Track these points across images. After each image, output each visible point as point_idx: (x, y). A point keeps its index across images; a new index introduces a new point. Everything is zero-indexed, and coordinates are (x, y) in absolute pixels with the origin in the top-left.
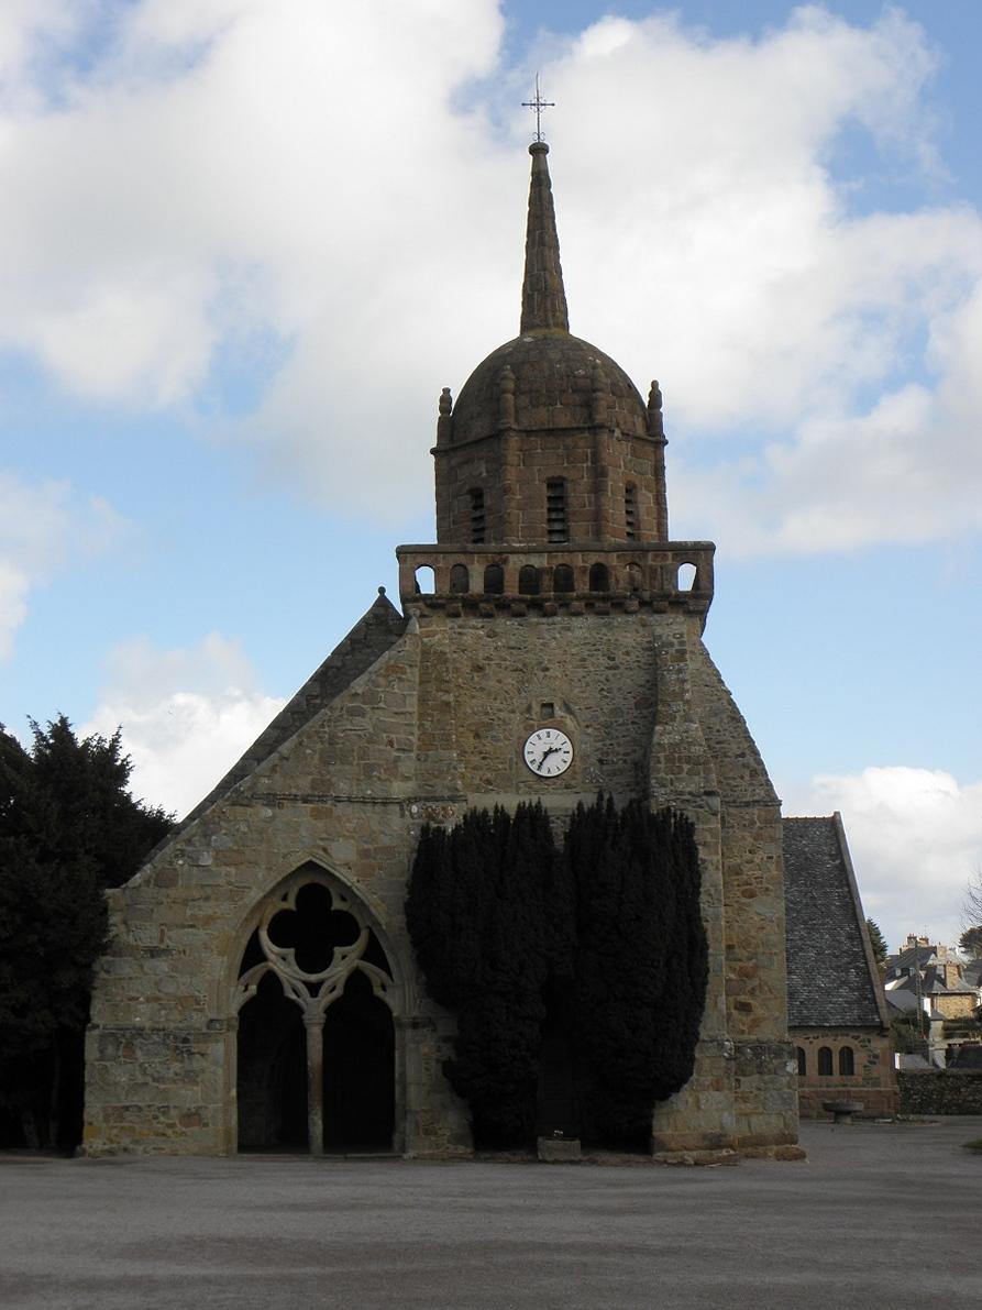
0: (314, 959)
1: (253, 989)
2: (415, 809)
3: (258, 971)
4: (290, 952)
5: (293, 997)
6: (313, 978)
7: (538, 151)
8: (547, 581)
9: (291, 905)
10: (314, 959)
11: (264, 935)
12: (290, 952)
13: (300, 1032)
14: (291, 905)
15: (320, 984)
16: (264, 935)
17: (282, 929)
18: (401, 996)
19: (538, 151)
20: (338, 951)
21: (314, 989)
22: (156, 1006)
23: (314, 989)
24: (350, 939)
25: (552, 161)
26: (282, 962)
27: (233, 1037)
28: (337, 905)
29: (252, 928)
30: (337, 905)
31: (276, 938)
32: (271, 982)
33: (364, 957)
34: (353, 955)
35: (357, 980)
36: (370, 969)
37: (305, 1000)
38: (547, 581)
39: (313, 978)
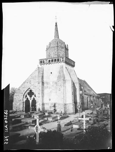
0: (31, 97)
3: (26, 98)
6: (31, 98)
7: (56, 24)
8: (51, 61)
9: (29, 92)
10: (31, 97)
14: (29, 92)
17: (28, 94)
19: (56, 24)
21: (31, 99)
22: (19, 100)
23: (31, 99)
24: (33, 95)
26: (28, 97)
27: (24, 103)
28: (32, 92)
30: (32, 92)
31: (28, 95)
36: (35, 97)
37: (30, 100)
38: (51, 61)
39: (31, 98)
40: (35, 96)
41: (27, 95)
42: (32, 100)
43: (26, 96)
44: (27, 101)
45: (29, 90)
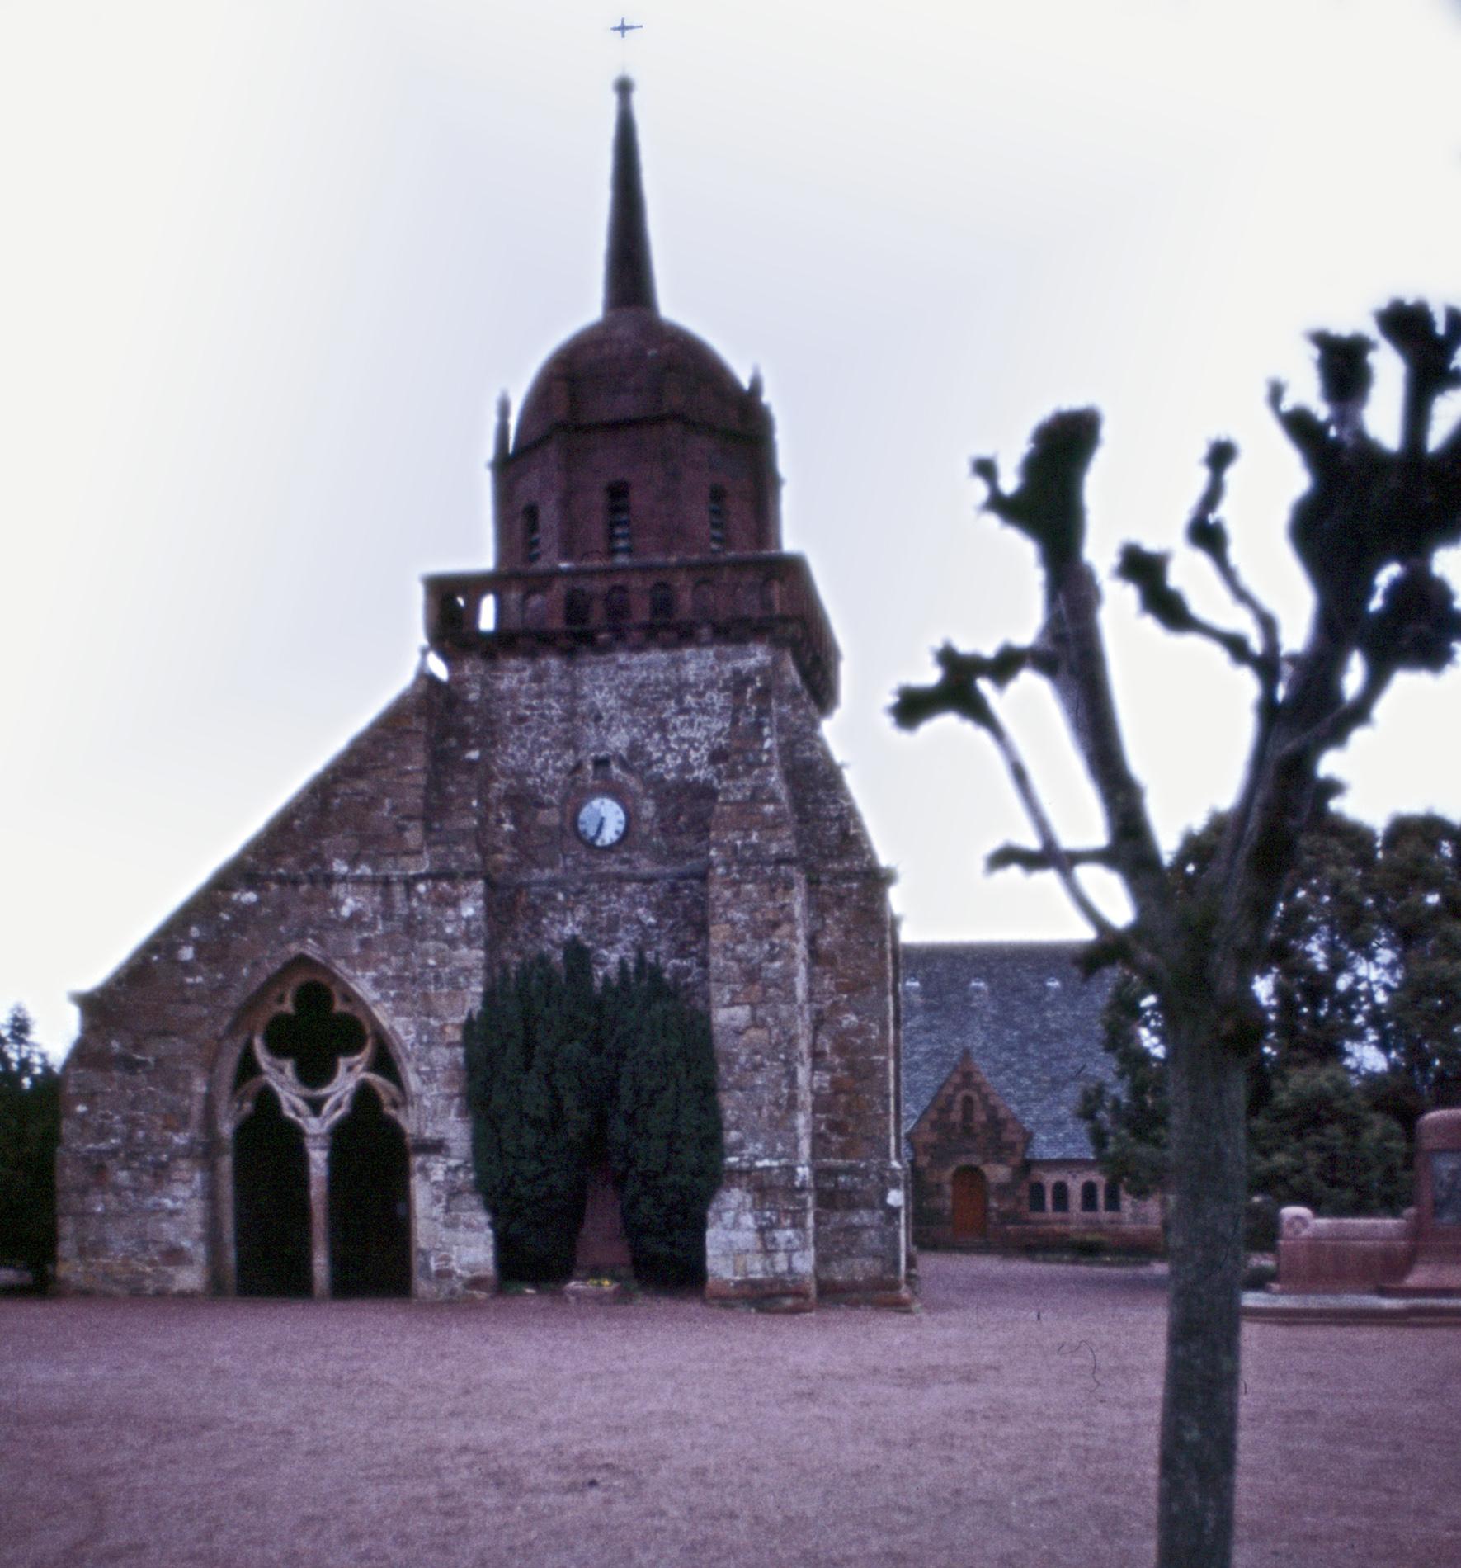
0: (315, 1073)
1: (248, 1106)
2: (421, 888)
3: (252, 1086)
4: (288, 1066)
5: (292, 1115)
7: (624, 88)
9: (288, 1007)
11: (258, 1044)
12: (288, 1066)
13: (303, 1160)
14: (288, 1007)
15: (323, 1100)
16: (258, 1044)
18: (434, 1111)
19: (624, 88)
20: (343, 1063)
21: (316, 1106)
24: (354, 1047)
25: (637, 99)
28: (339, 1007)
29: (241, 1039)
30: (339, 1007)
31: (277, 1049)
32: (267, 1100)
33: (369, 1069)
34: (360, 1067)
35: (364, 1096)
40: (385, 1062)
41: (263, 1058)
42: (332, 1115)
43: (248, 1067)
44: (267, 1142)
45: (300, 978)
